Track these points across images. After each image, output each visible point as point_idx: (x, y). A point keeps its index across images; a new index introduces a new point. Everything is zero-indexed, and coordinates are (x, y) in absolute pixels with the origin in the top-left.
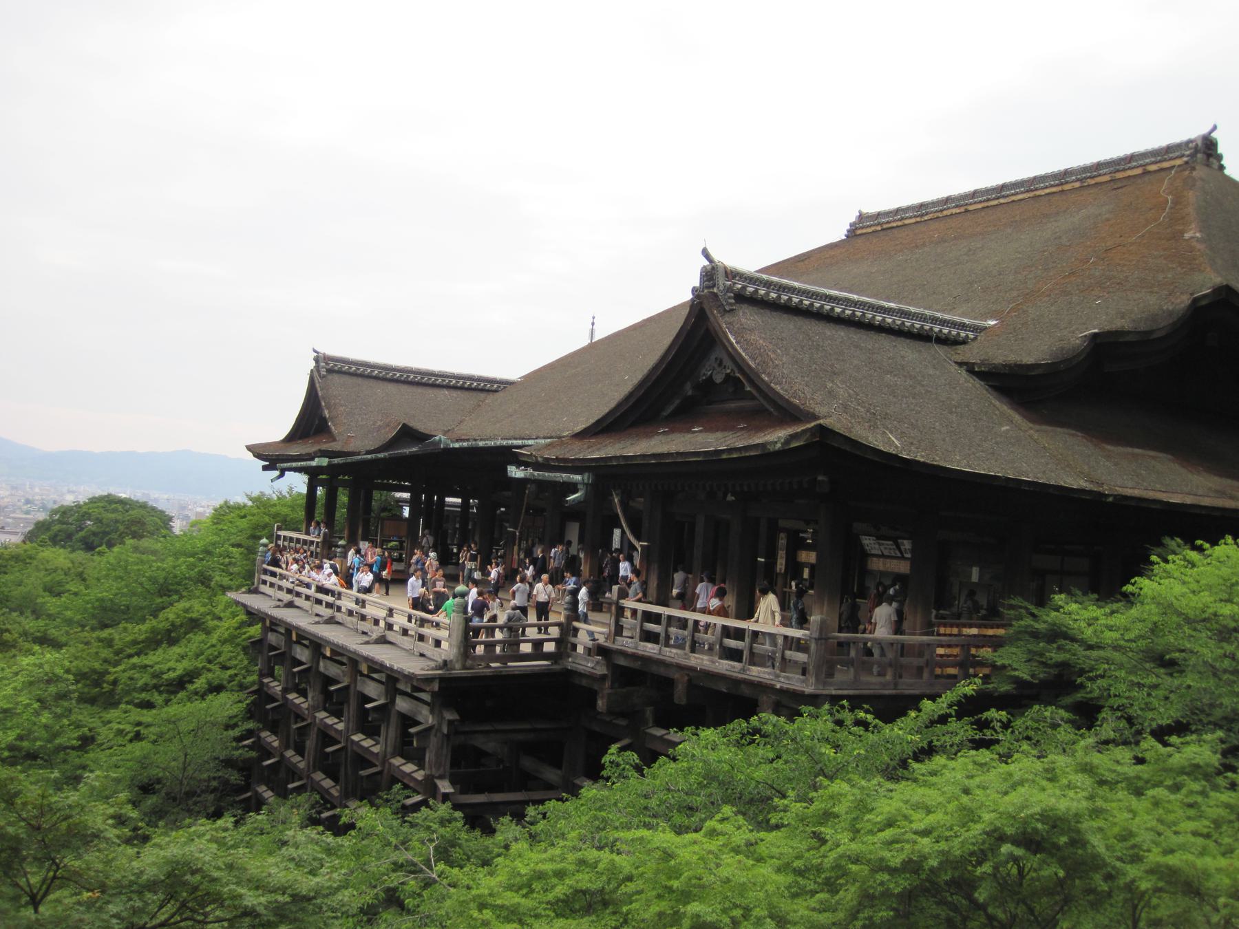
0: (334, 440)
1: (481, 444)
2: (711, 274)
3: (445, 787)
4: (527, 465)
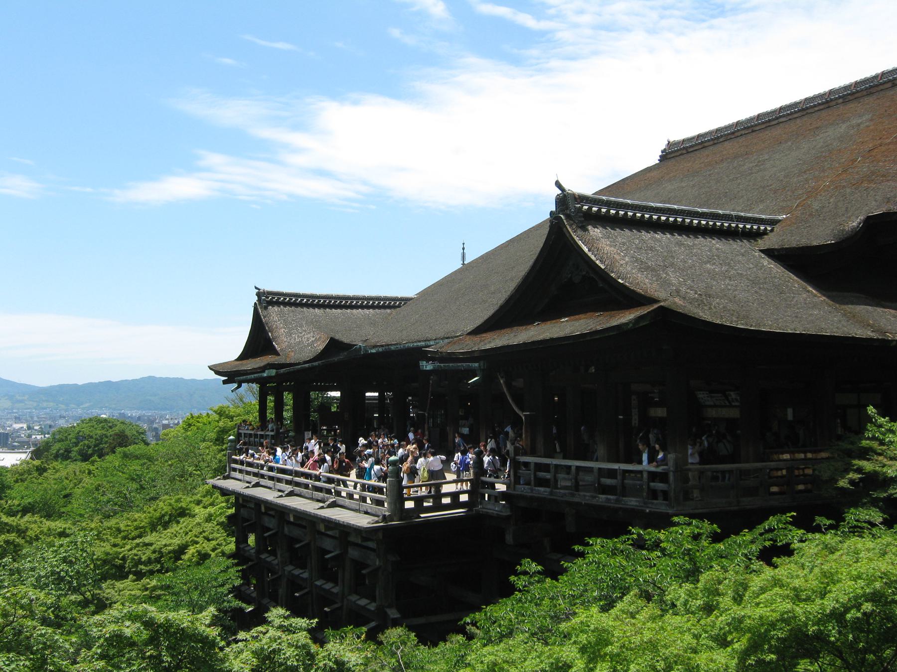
0: (278, 354)
2: (565, 200)
3: (393, 613)
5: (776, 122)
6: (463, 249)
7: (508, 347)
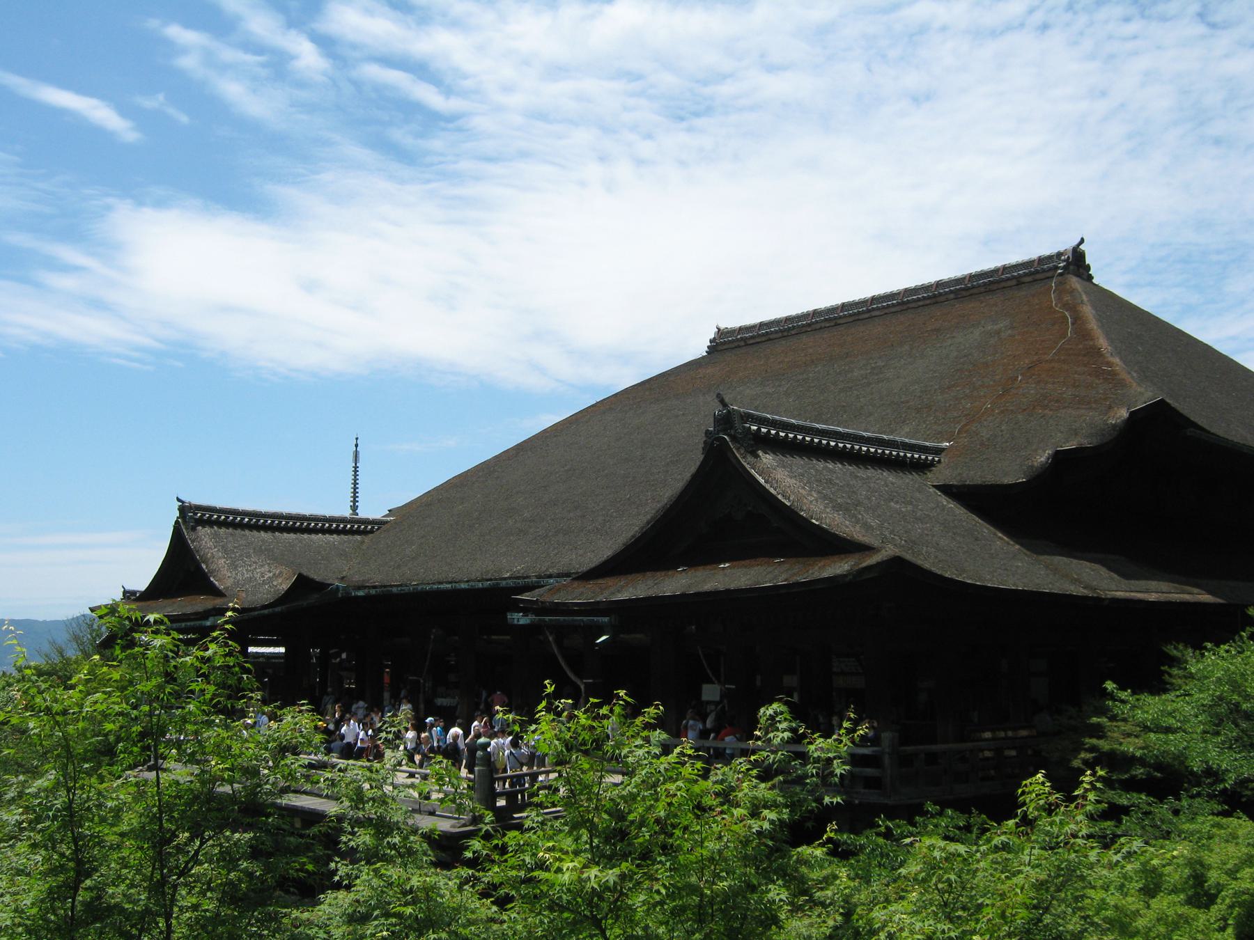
4: (526, 611)
5: (866, 316)
7: (657, 597)
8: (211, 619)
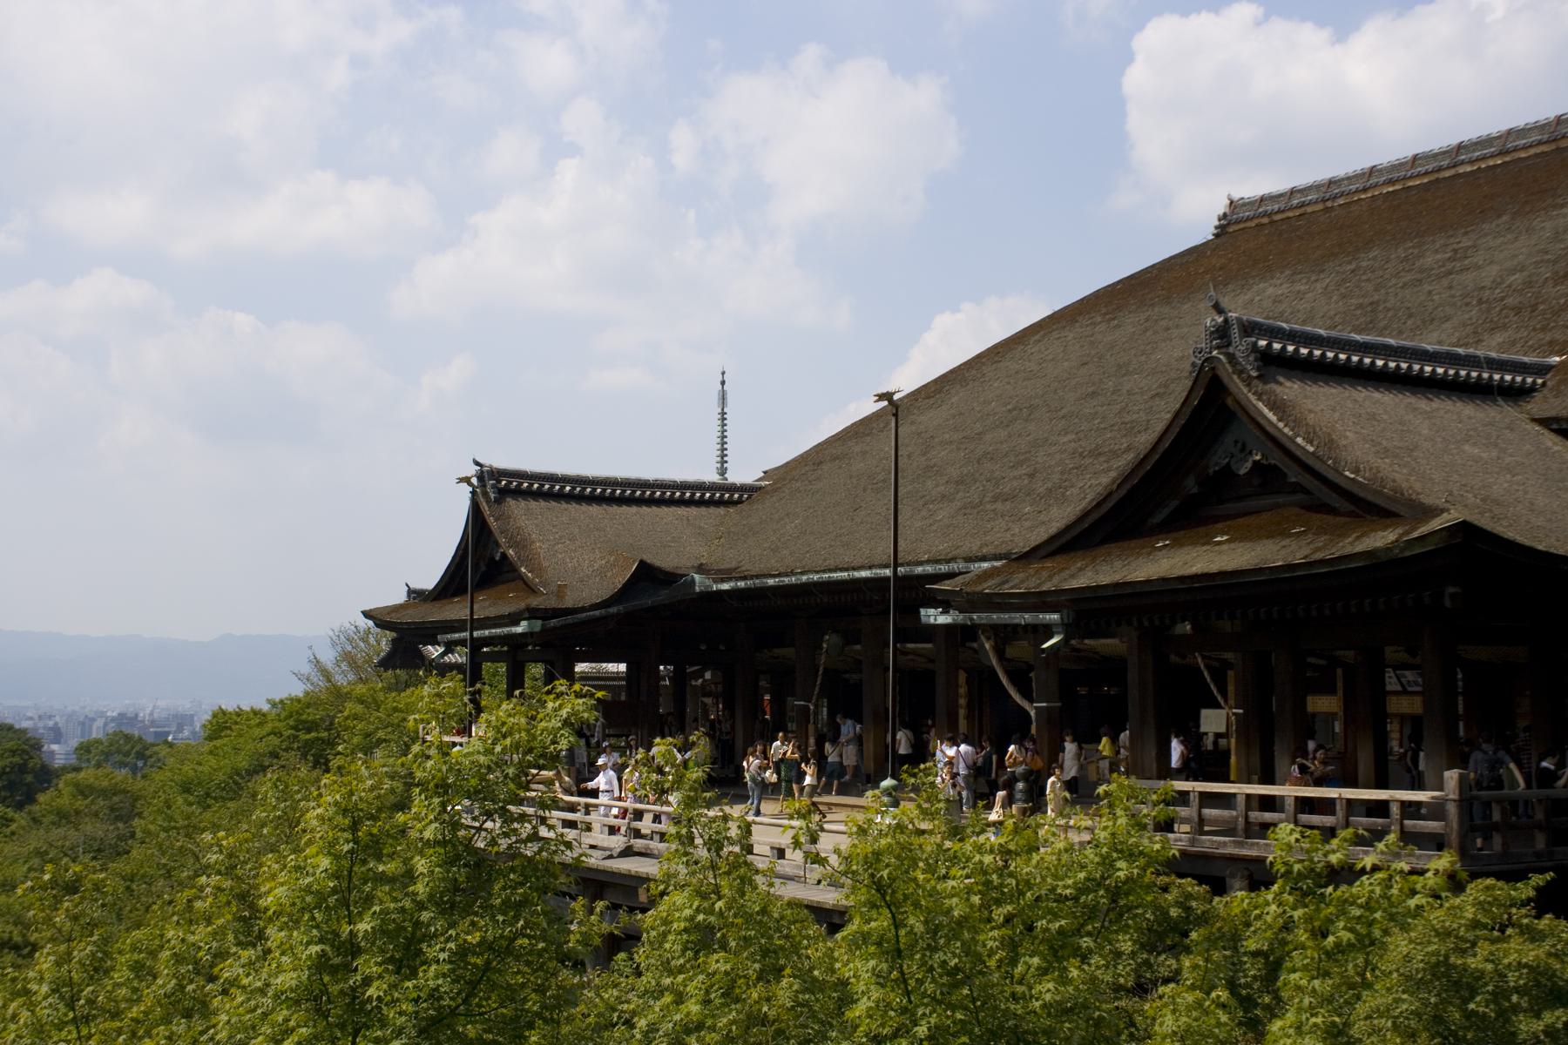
1: (771, 582)
4: (946, 606)
6: (723, 383)
8: (524, 623)
